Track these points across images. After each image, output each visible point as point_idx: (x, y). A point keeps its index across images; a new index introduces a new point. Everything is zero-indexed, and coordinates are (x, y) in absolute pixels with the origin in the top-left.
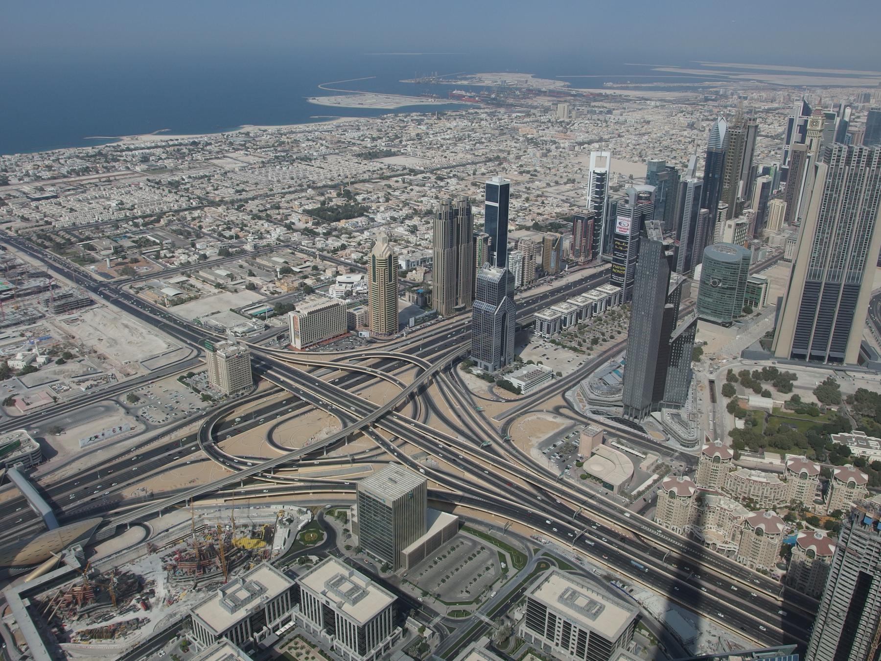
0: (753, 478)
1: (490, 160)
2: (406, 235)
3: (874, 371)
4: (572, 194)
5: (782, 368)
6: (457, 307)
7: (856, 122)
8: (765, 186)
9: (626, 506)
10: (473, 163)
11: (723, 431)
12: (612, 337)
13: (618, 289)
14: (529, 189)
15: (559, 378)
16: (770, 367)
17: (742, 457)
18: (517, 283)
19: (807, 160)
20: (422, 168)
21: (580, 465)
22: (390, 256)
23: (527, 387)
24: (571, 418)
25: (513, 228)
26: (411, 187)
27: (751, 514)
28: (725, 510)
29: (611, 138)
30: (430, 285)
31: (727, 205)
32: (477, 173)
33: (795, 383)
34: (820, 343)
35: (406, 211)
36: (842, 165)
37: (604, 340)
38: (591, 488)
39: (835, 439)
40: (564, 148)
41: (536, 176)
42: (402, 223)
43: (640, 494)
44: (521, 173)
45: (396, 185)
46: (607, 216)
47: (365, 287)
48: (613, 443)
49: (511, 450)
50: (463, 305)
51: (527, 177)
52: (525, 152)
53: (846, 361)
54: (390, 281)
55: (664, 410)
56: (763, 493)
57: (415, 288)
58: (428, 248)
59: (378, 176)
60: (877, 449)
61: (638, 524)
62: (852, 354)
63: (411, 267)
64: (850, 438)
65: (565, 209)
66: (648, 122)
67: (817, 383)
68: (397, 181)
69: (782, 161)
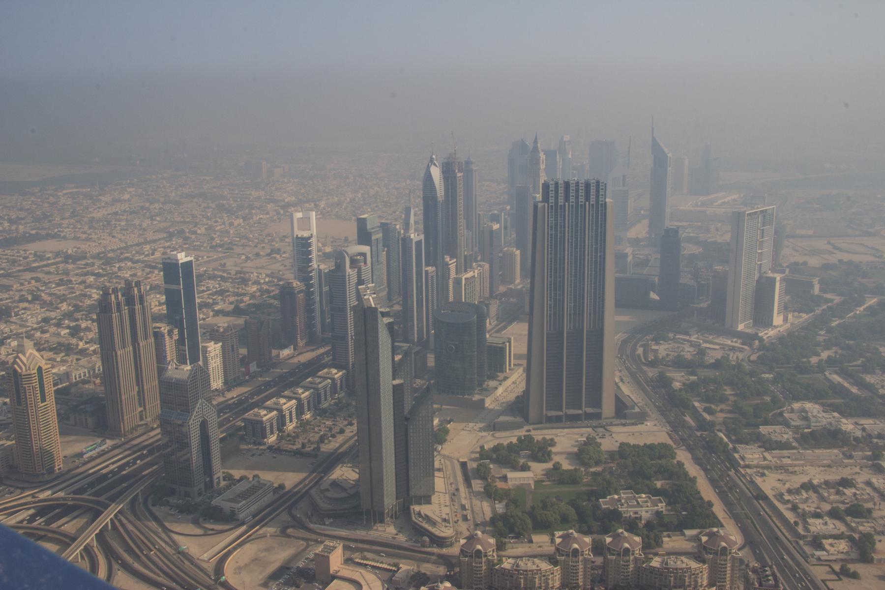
1: (171, 236)
3: (632, 421)
4: (278, 266)
5: (538, 435)
6: (143, 422)
12: (342, 431)
13: (344, 371)
15: (282, 492)
16: (525, 436)
17: (508, 546)
18: (217, 383)
22: (40, 369)
24: (303, 539)
31: (455, 260)
33: (554, 449)
37: (333, 436)
39: (604, 503)
41: (232, 249)
42: (59, 325)
45: (46, 278)
47: (10, 415)
48: (357, 560)
52: (216, 222)
53: (604, 416)
54: (43, 399)
59: (21, 268)
60: (648, 507)
62: (608, 407)
64: (619, 500)
68: (49, 273)
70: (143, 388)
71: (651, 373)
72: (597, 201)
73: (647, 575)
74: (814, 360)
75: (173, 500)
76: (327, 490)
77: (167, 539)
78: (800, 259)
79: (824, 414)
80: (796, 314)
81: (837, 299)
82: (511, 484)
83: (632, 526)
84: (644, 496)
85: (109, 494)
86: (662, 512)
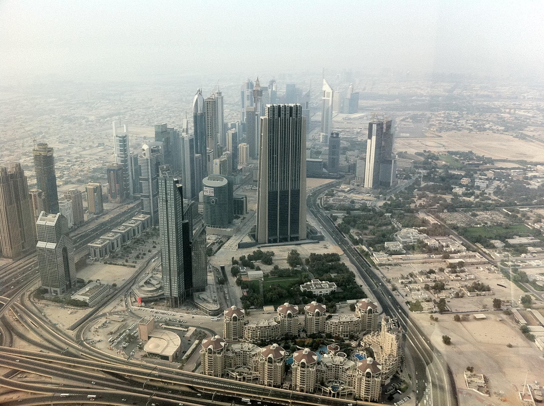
3: (317, 241)
4: (102, 154)
6: (24, 250)
7: (281, 92)
8: (234, 136)
9: (181, 368)
11: (236, 299)
12: (149, 251)
13: (149, 216)
14: (69, 153)
16: (257, 251)
19: (256, 117)
21: (141, 348)
23: (91, 299)
25: (61, 183)
27: (264, 349)
28: (246, 352)
31: (212, 150)
33: (274, 258)
34: (284, 232)
36: (276, 116)
37: (144, 254)
38: (153, 363)
41: (73, 143)
43: (189, 357)
46: (132, 166)
49: (87, 351)
50: (27, 248)
51: (66, 145)
56: (268, 334)
61: (190, 379)
62: (303, 233)
64: (311, 285)
65: (100, 166)
66: (151, 100)
67: (286, 255)
69: (242, 119)
71: (325, 213)
72: (297, 117)
75: (47, 296)
76: (143, 286)
78: (404, 150)
80: (402, 180)
81: (423, 172)
82: (250, 279)
83: (319, 299)
84: (323, 282)
85: (4, 295)
86: (335, 291)
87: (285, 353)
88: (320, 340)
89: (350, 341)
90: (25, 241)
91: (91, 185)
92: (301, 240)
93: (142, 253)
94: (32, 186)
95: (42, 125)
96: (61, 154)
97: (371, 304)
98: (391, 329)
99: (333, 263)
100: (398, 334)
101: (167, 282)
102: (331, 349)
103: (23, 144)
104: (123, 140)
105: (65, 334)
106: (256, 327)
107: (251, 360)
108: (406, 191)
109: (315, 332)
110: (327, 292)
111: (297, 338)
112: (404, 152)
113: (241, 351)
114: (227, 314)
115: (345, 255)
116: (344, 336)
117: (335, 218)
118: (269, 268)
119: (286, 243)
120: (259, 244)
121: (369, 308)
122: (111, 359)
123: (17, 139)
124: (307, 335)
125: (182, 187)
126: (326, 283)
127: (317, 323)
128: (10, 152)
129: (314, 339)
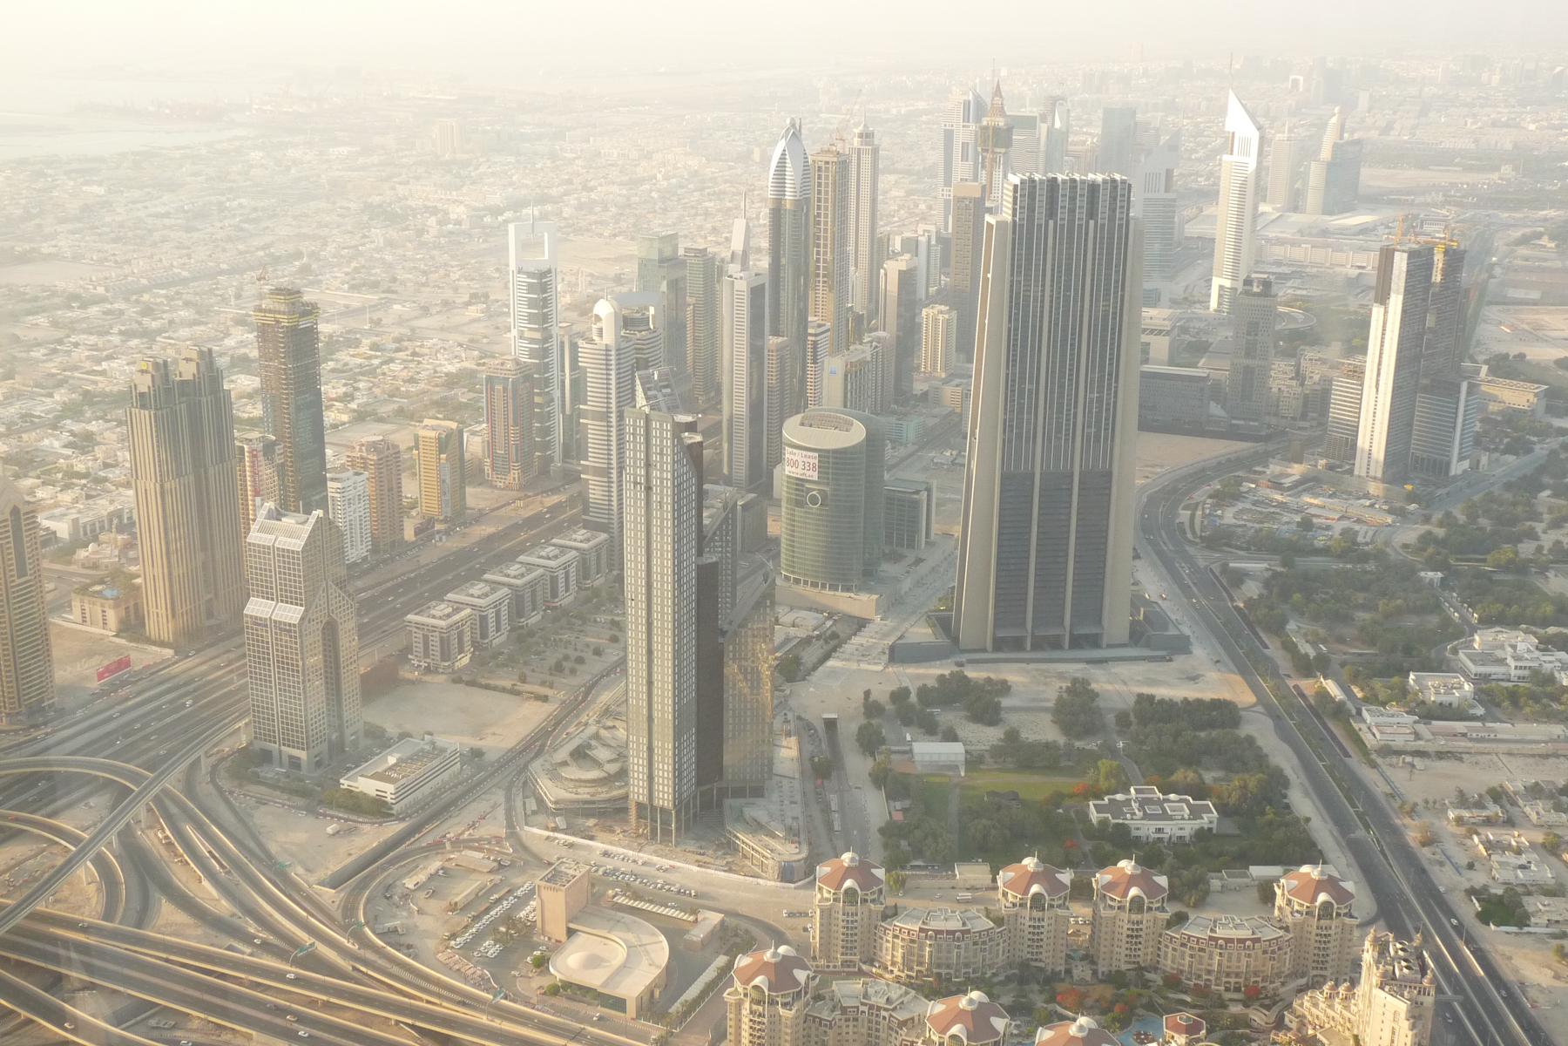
0: (935, 925)
2: (67, 457)
6: (212, 622)
8: (906, 279)
10: (233, 271)
12: (598, 652)
13: (604, 536)
14: (378, 322)
16: (952, 674)
20: (101, 290)
21: (542, 964)
22: (15, 511)
23: (400, 794)
25: (345, 418)
26: (73, 339)
27: (937, 1007)
28: (879, 1009)
29: (566, 194)
30: (138, 576)
31: (828, 325)
32: (245, 294)
33: (1006, 702)
35: (61, 396)
37: (580, 660)
40: (458, 222)
42: (55, 427)
44: (353, 288)
48: (621, 900)
51: (374, 297)
52: (364, 236)
53: (1105, 642)
55: (729, 802)
56: (958, 956)
57: (98, 588)
58: (127, 485)
60: (1183, 819)
62: (1117, 622)
63: (87, 534)
64: (1129, 801)
67: (1052, 692)
69: (941, 224)
70: (213, 556)
72: (1112, 219)
73: (1174, 949)
74: (1526, 549)
75: (268, 772)
76: (565, 764)
77: (257, 850)
78: (1513, 350)
79: (1537, 654)
80: (1496, 455)
83: (1151, 856)
84: (1172, 796)
85: (139, 761)
86: (1210, 829)
87: (1007, 1026)
88: (1140, 995)
89: (1246, 1006)
90: (216, 595)
91: (431, 428)
92: (1110, 646)
93: (573, 654)
94: (253, 423)
95: (304, 230)
96: (352, 323)
97: (1330, 884)
98: (1394, 978)
99: (1214, 733)
100: (1421, 998)
101: (638, 757)
102: (1177, 1028)
103: (240, 289)
104: (542, 284)
105: (309, 899)
106: (921, 930)
107: (892, 1039)
108: (1508, 496)
109: (1124, 967)
110: (1180, 833)
111: (1063, 980)
112: (1515, 357)
113: (863, 1004)
114: (826, 880)
115: (1260, 708)
116: (1227, 990)
117: (1238, 578)
118: (990, 736)
119: (1056, 654)
120: (963, 651)
121: (1323, 897)
122: (445, 993)
123: (221, 273)
124: (1095, 972)
125: (700, 444)
126: (1180, 801)
127: (1134, 936)
128: (198, 313)
129: (1118, 989)
